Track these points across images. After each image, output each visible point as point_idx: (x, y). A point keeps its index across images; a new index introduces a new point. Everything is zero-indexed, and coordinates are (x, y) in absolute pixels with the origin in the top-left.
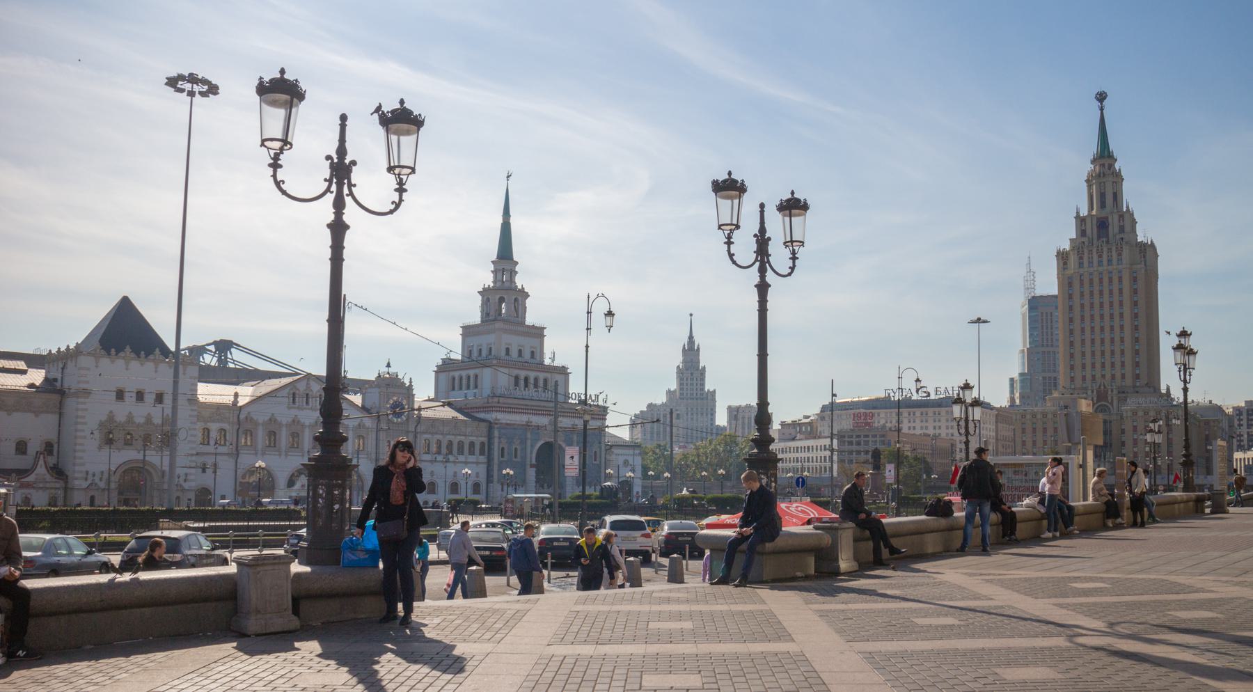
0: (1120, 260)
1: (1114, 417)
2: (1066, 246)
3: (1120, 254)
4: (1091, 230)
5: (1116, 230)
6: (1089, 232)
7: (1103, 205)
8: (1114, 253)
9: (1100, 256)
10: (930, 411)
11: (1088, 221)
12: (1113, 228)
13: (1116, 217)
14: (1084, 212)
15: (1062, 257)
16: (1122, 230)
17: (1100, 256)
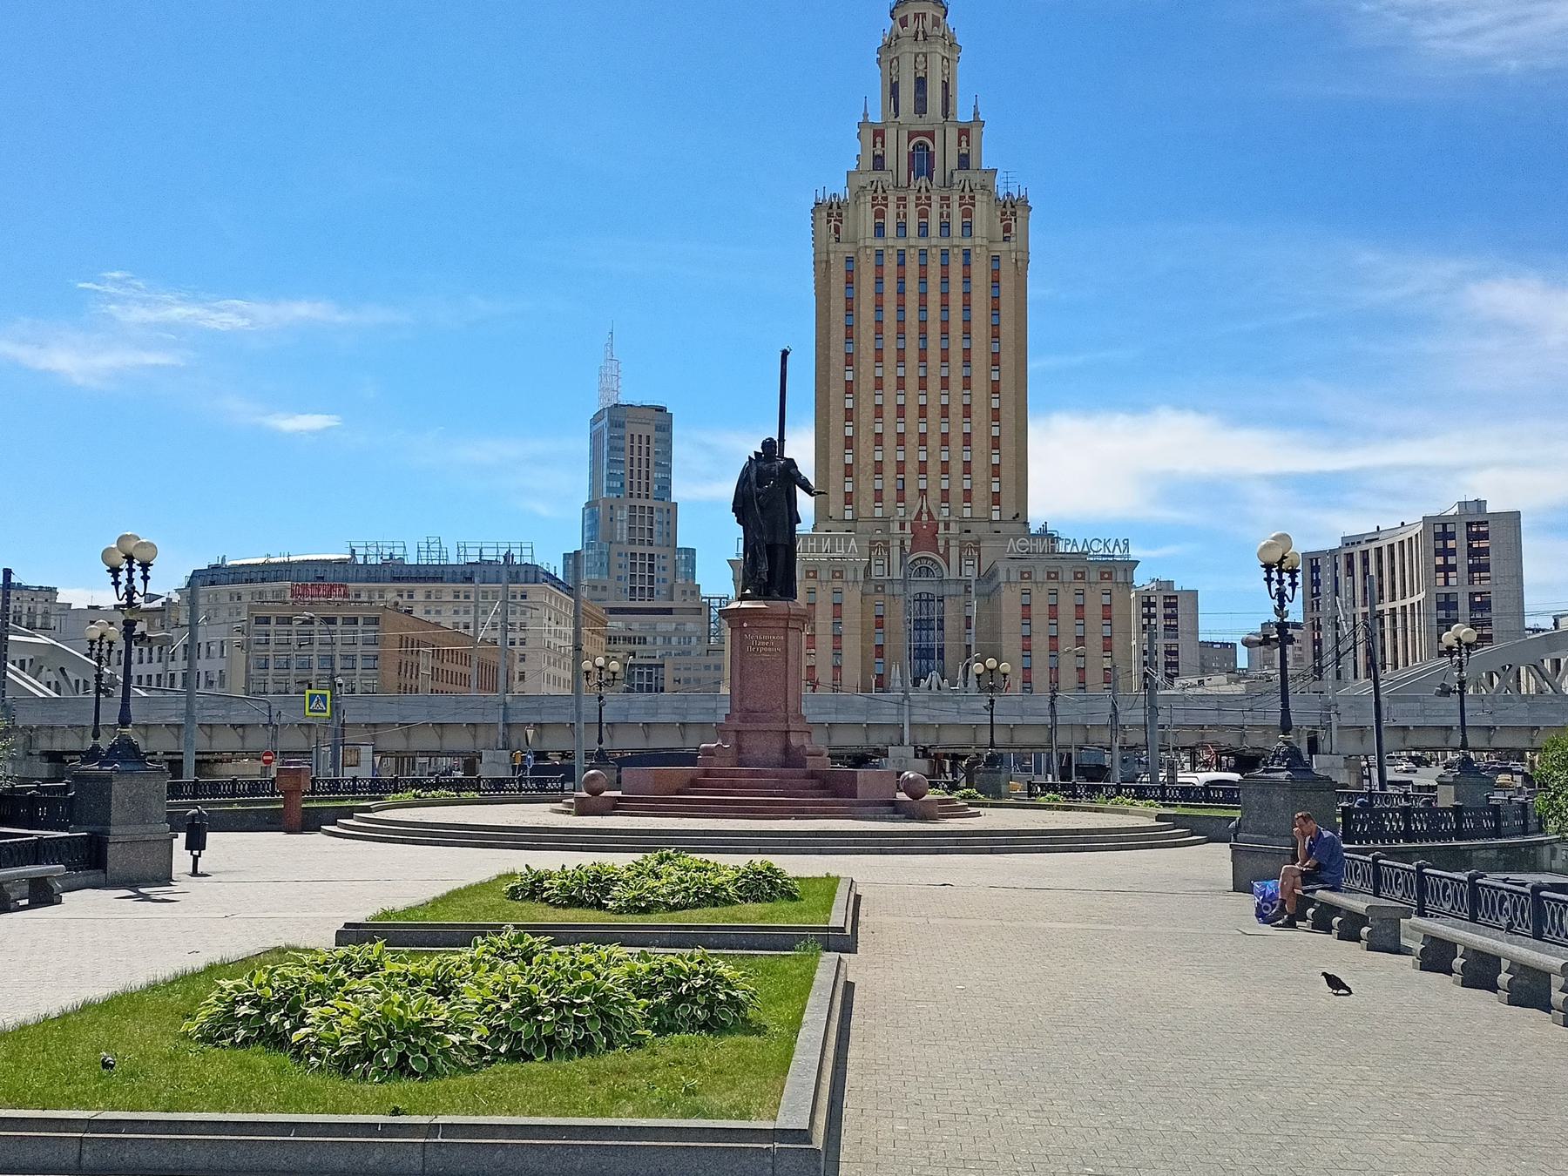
0: (967, 227)
1: (950, 589)
2: (839, 188)
3: (967, 214)
4: (897, 150)
5: (953, 162)
6: (890, 162)
7: (921, 107)
8: (956, 211)
9: (923, 214)
10: (448, 588)
11: (890, 134)
12: (946, 152)
13: (952, 135)
14: (876, 117)
15: (830, 213)
16: (964, 162)
17: (923, 214)
